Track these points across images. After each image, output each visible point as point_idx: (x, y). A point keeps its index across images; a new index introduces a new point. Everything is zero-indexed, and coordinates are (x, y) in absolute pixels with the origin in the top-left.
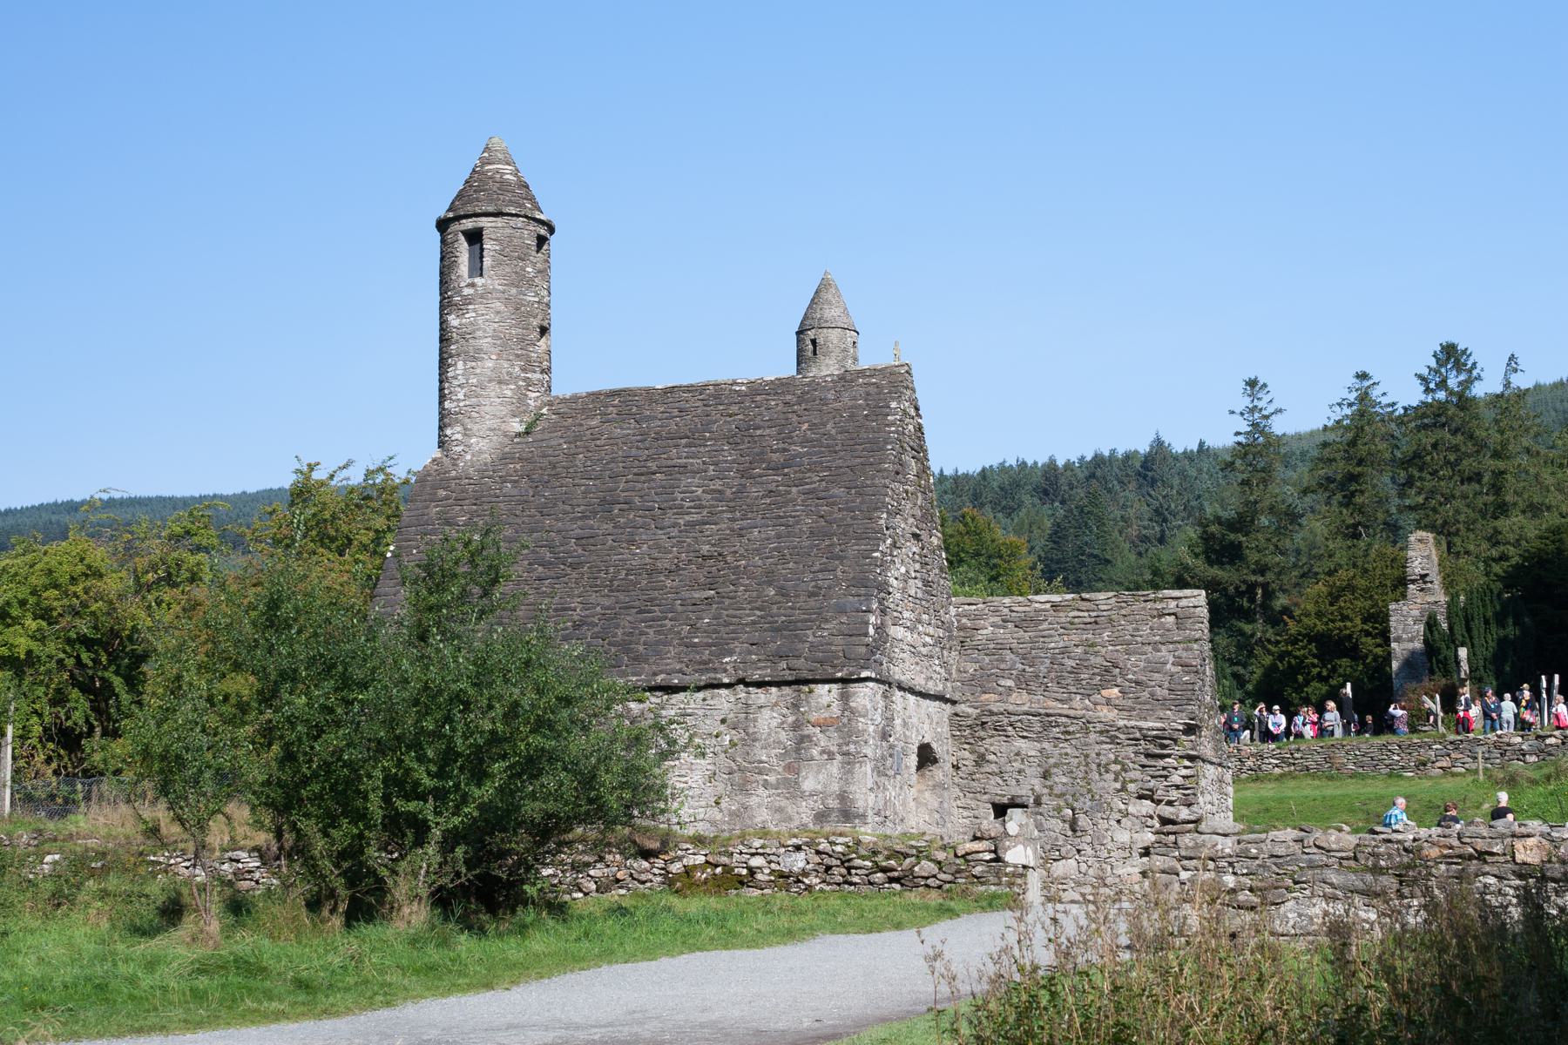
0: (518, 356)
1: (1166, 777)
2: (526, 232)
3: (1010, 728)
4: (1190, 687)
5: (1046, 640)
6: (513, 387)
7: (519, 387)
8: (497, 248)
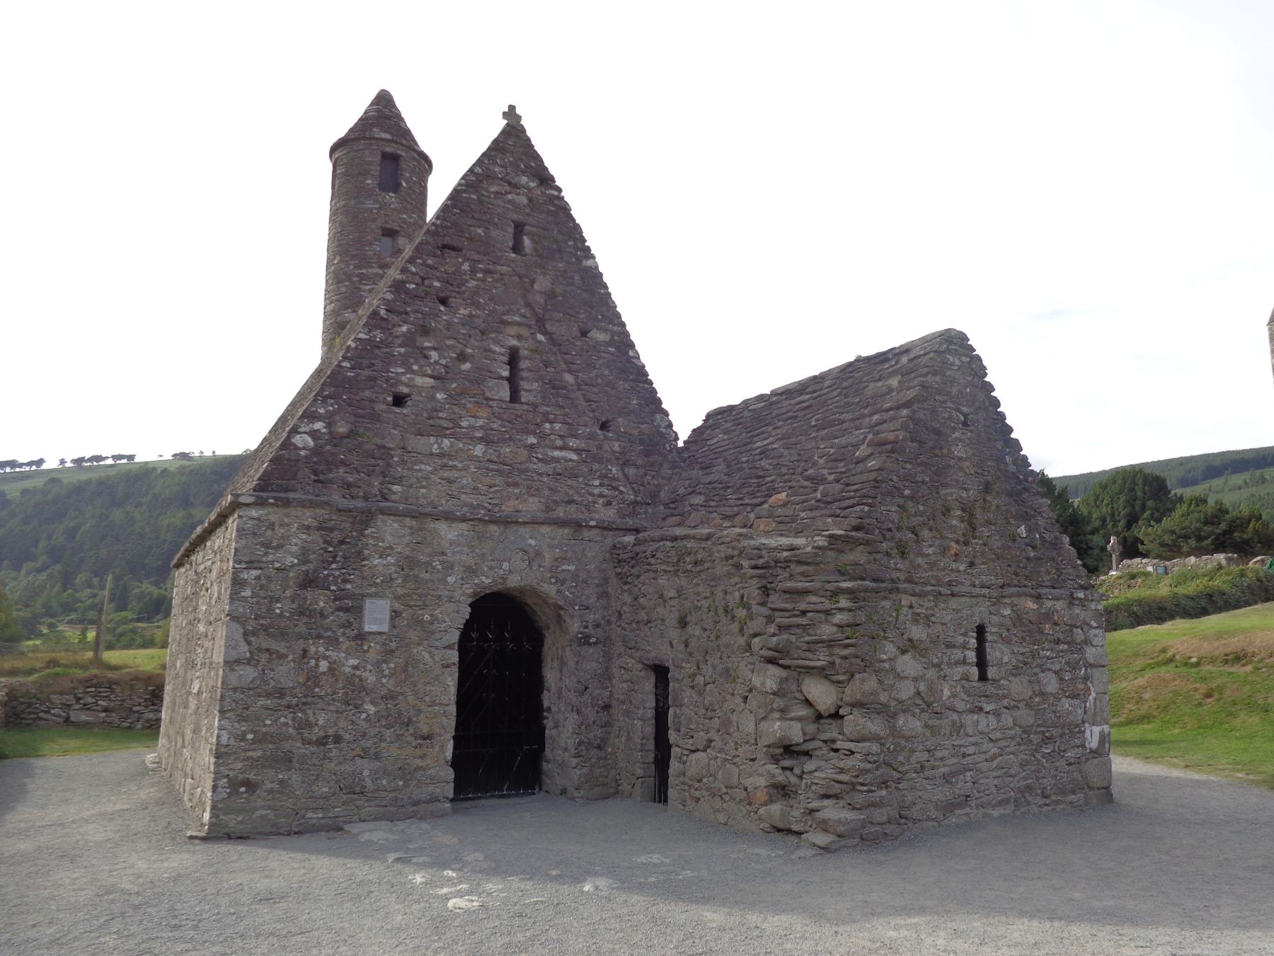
1: (804, 627)
3: (652, 561)
4: (872, 476)
5: (755, 439)
6: (347, 283)
7: (353, 283)
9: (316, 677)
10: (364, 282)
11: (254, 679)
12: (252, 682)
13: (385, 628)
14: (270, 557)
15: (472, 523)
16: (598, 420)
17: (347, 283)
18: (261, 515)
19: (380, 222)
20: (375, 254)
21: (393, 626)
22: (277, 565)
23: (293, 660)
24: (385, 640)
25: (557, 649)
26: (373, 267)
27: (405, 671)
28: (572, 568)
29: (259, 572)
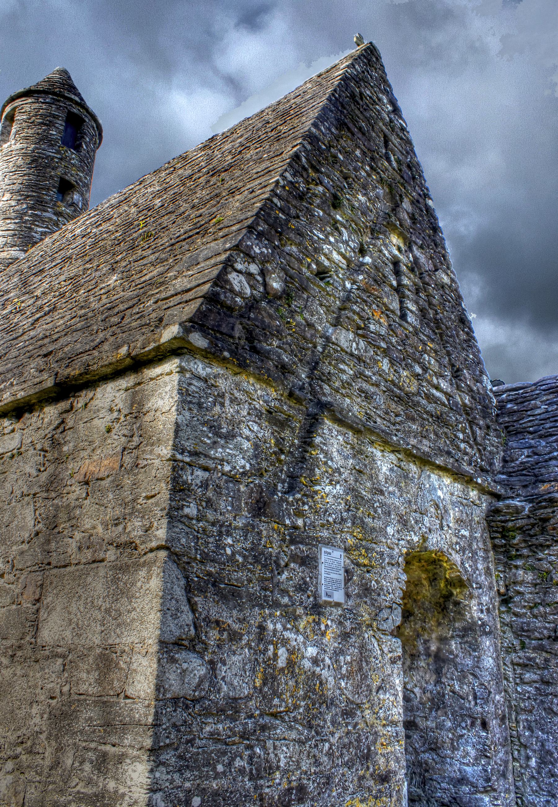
0: (28, 196)
2: (53, 106)
8: (25, 117)
9: (274, 678)
10: (37, 223)
11: (201, 681)
12: (199, 685)
13: (339, 596)
14: (219, 453)
15: (399, 456)
16: (453, 366)
17: (17, 221)
18: (208, 375)
19: (60, 171)
20: (52, 200)
21: (348, 595)
22: (227, 468)
23: (248, 645)
24: (340, 616)
25: (426, 642)
26: (47, 211)
27: (360, 669)
28: (467, 533)
29: (206, 475)
